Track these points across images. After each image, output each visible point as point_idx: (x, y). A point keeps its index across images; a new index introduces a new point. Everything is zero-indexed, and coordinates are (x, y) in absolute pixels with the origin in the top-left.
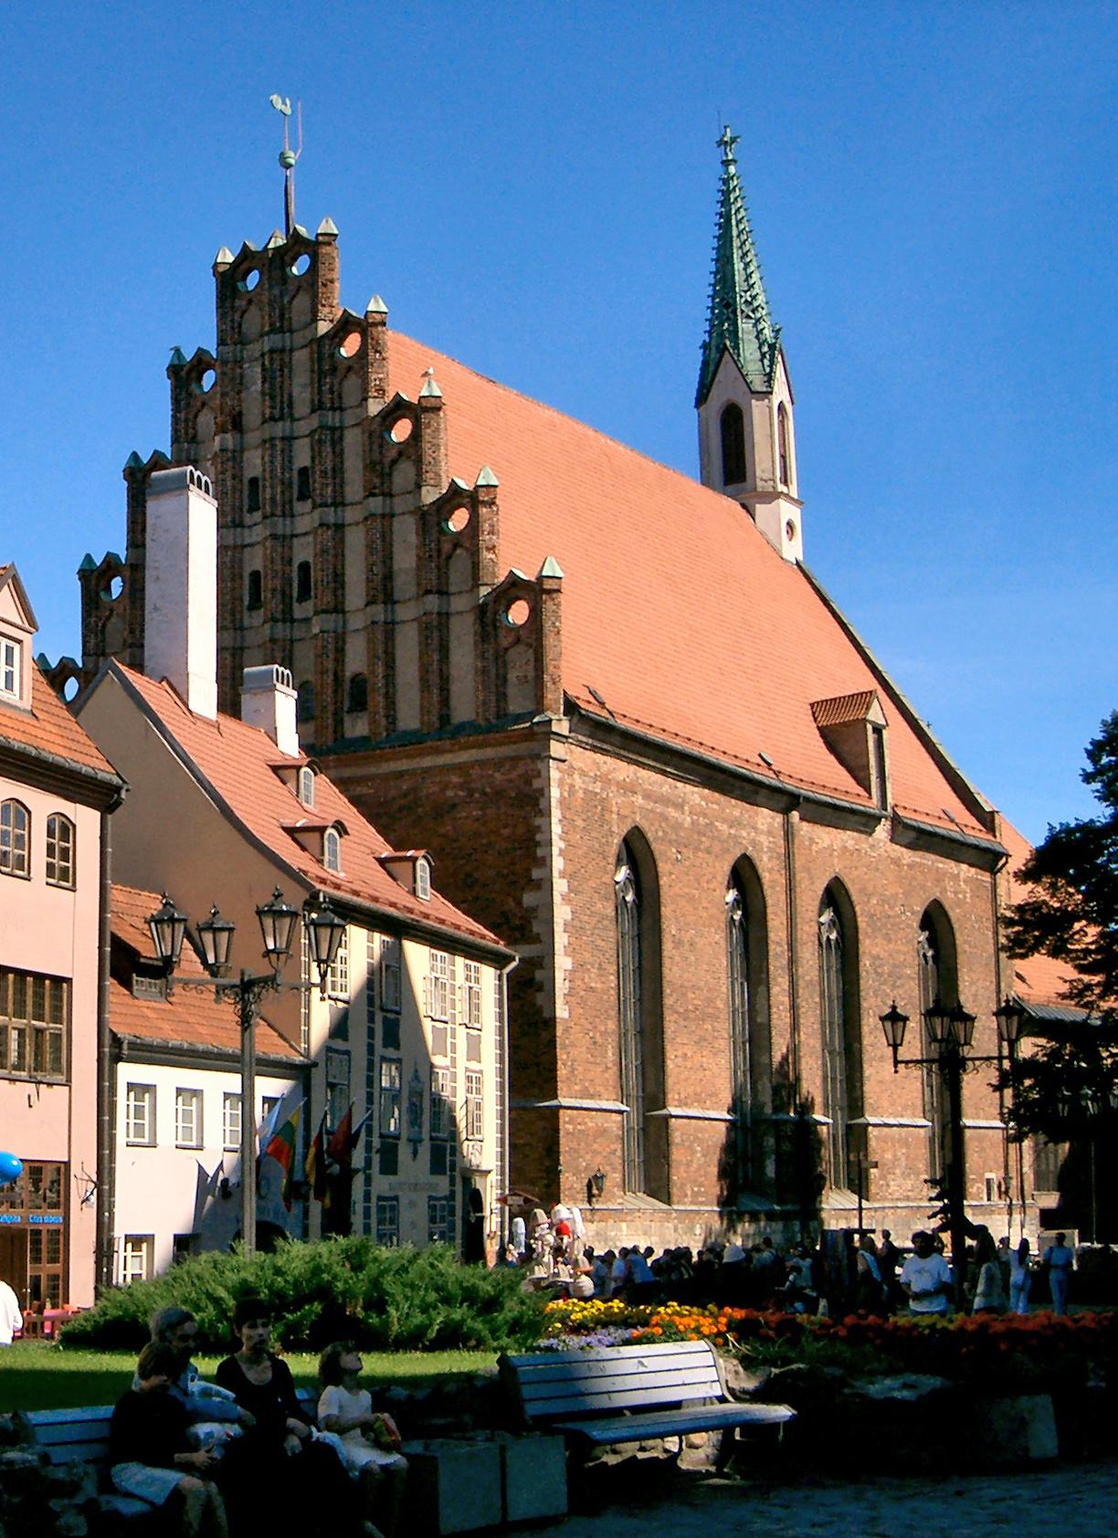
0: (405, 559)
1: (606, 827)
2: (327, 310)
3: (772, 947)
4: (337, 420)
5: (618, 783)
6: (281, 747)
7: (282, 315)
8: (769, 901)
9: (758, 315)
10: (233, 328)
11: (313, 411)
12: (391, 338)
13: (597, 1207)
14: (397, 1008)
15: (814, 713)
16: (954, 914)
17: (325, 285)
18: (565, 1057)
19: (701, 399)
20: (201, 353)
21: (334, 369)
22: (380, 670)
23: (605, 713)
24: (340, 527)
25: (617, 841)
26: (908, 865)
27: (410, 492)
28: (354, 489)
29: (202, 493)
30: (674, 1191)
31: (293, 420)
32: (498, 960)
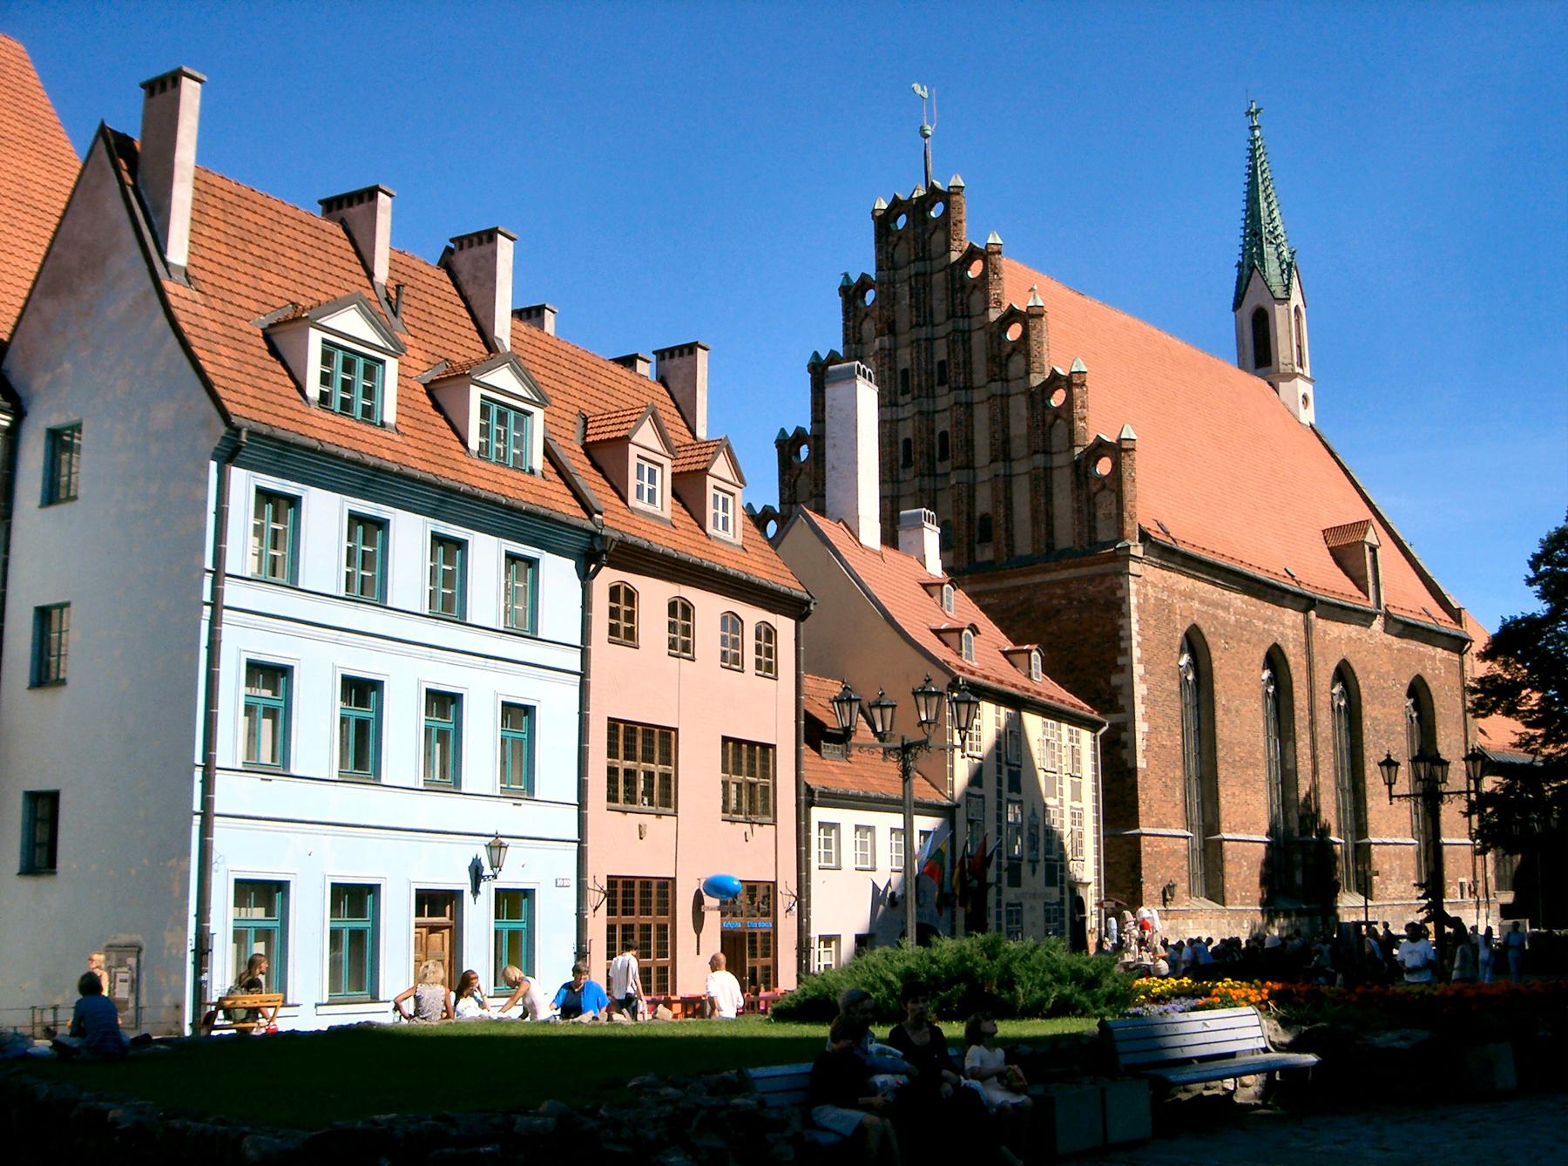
0: (1019, 428)
1: (1172, 625)
2: (957, 243)
3: (1297, 712)
4: (966, 325)
5: (1180, 592)
6: (929, 570)
7: (924, 247)
8: (1295, 678)
9: (1279, 241)
10: (887, 258)
11: (948, 319)
12: (1005, 263)
13: (1170, 908)
14: (1018, 763)
15: (1325, 538)
16: (1432, 685)
17: (955, 225)
18: (1144, 797)
19: (1237, 304)
20: (864, 277)
21: (963, 287)
22: (1002, 511)
23: (1170, 540)
24: (970, 405)
25: (1180, 635)
26: (1398, 650)
27: (1021, 378)
28: (980, 376)
29: (867, 381)
30: (1228, 895)
31: (934, 325)
32: (1093, 726)
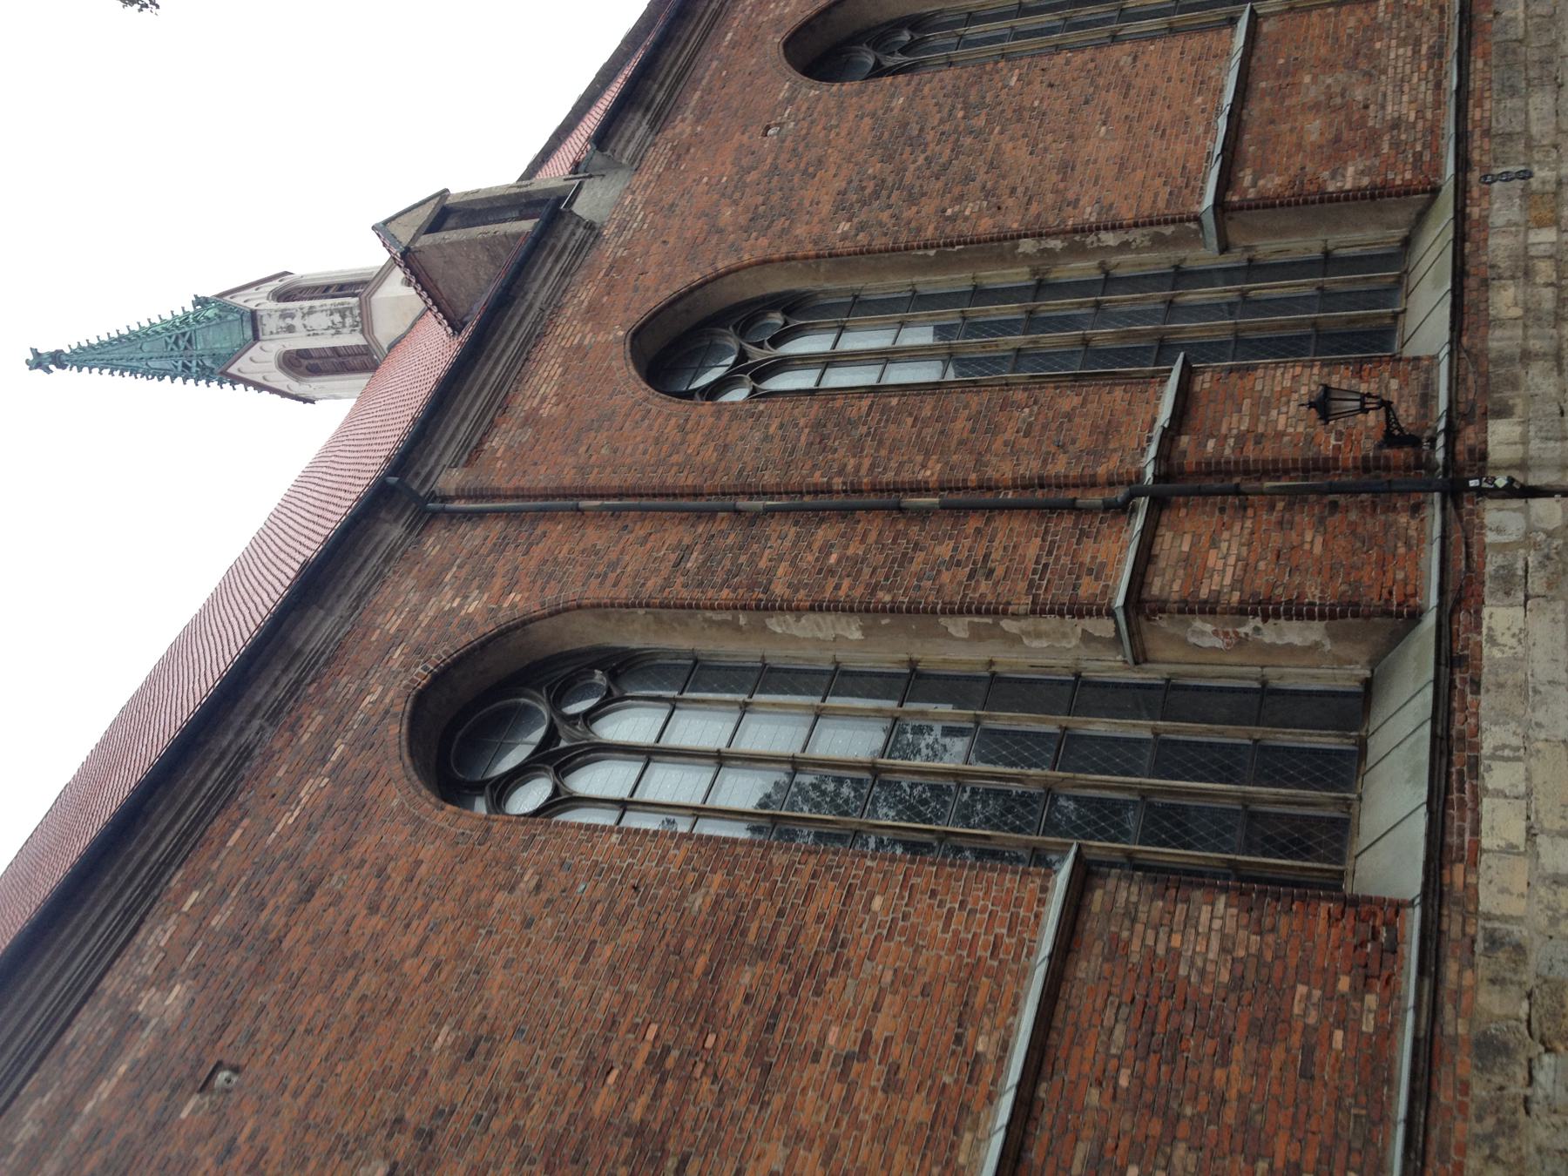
26: (698, 121)
